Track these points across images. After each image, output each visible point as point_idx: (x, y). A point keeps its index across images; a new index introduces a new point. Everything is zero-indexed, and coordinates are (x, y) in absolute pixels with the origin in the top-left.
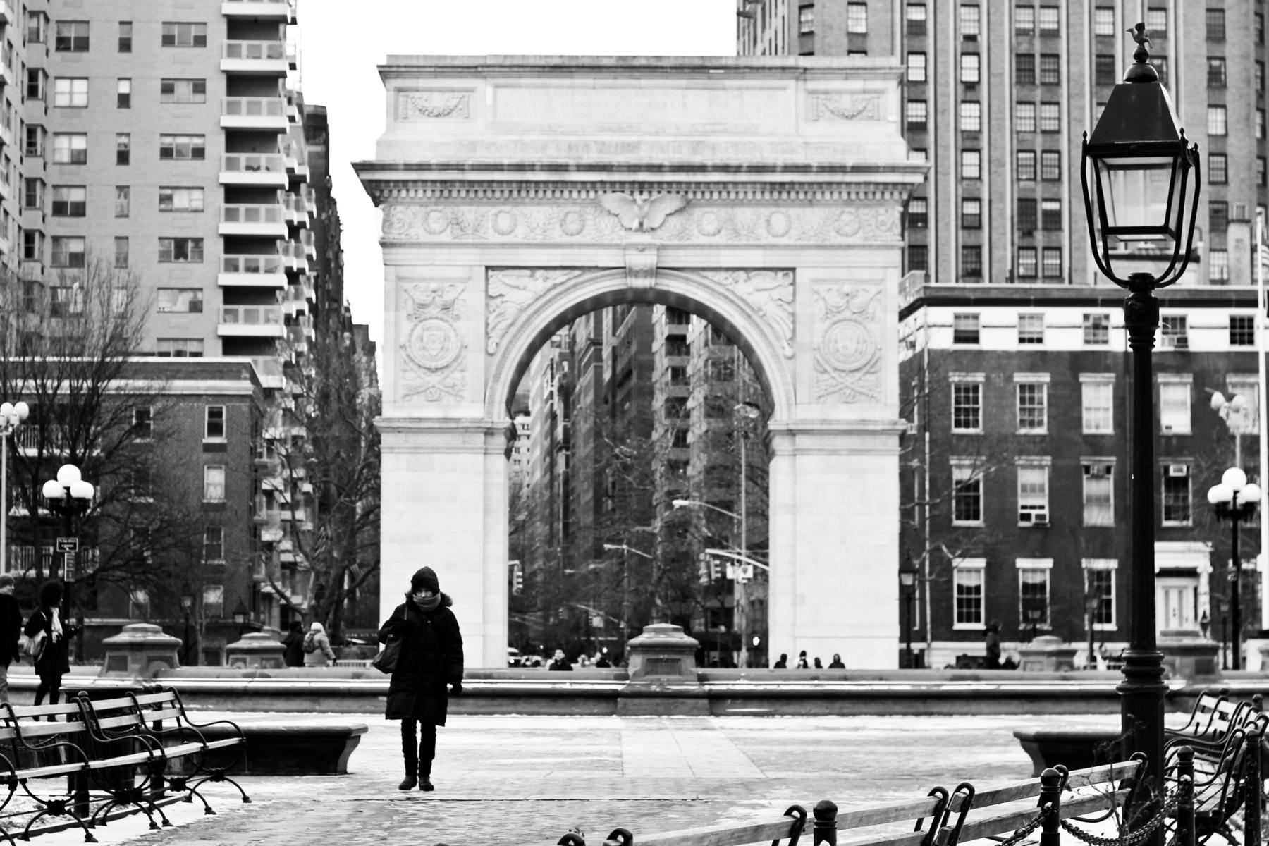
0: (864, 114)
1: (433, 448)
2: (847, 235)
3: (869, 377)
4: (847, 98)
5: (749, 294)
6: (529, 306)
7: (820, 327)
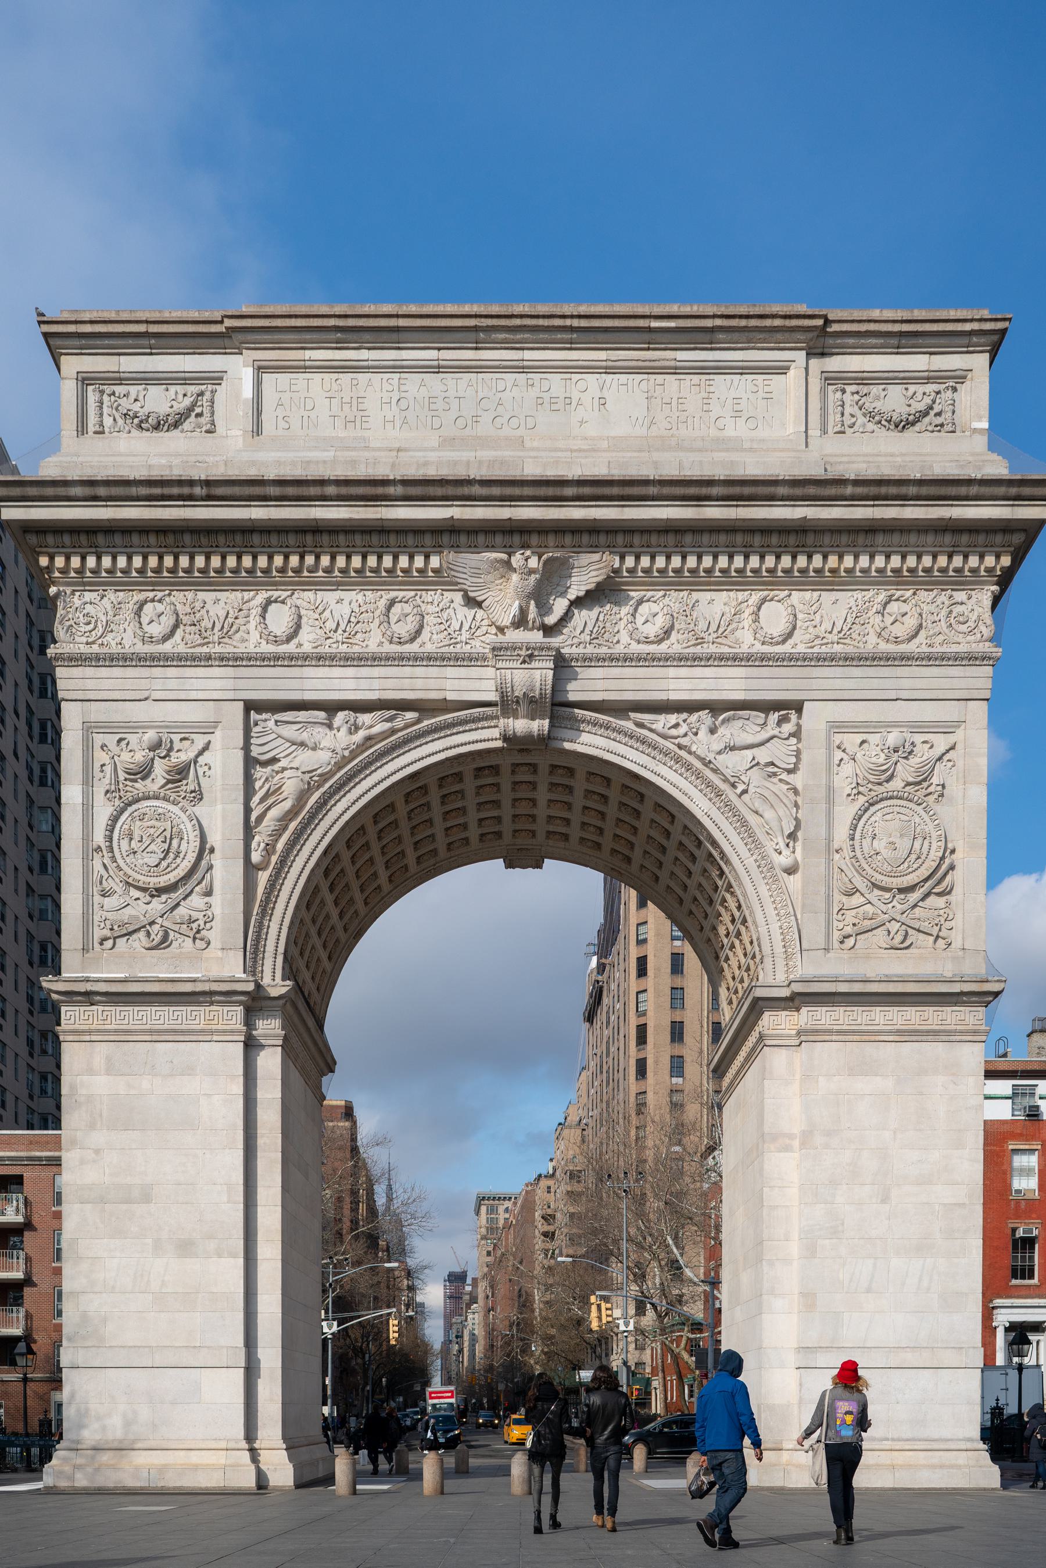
0: (926, 420)
1: (151, 1032)
2: (897, 641)
3: (932, 900)
4: (895, 391)
5: (719, 753)
6: (330, 774)
7: (845, 812)
